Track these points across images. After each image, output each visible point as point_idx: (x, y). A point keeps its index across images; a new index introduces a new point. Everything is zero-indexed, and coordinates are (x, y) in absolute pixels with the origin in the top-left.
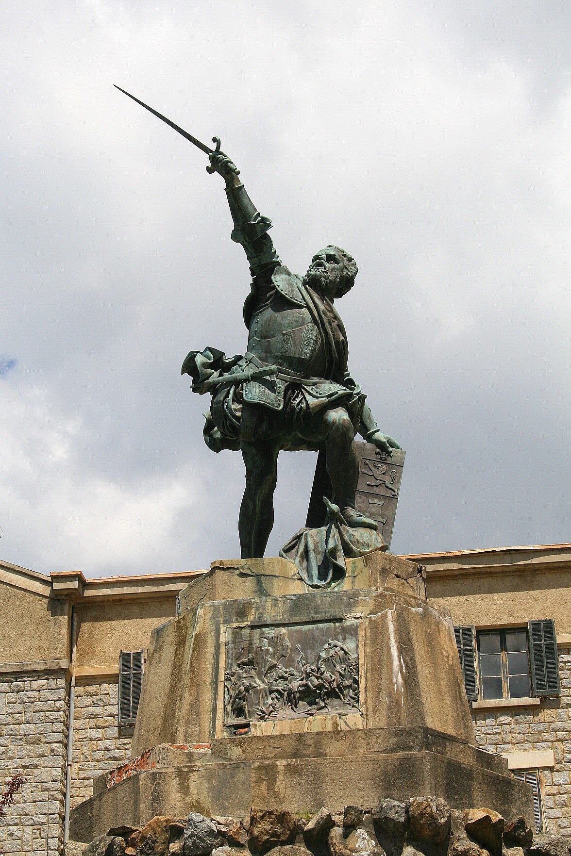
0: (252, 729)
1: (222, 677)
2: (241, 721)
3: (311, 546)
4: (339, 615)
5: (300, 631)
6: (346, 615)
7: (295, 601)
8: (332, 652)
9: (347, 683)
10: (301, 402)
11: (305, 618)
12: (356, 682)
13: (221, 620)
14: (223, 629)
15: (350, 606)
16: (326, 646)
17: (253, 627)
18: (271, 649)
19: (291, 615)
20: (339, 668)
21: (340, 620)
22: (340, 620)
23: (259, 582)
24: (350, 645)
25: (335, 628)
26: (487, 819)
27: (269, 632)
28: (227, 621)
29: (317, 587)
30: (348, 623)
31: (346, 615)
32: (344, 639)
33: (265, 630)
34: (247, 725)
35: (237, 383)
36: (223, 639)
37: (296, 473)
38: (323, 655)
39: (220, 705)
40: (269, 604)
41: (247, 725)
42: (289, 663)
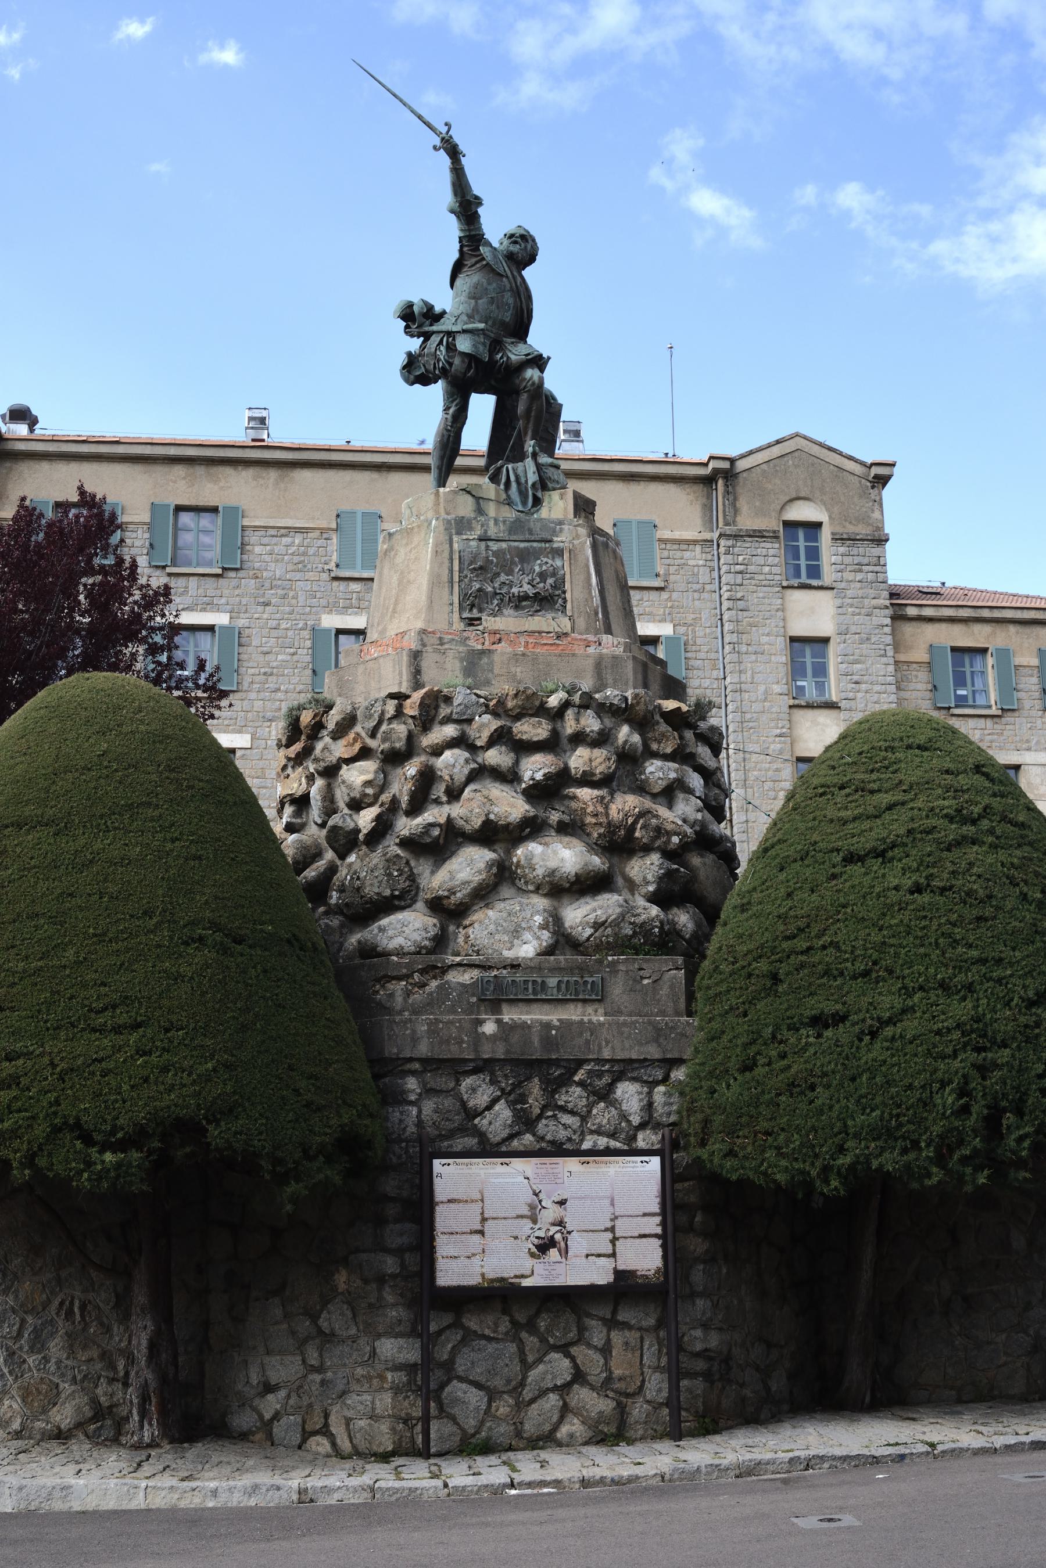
0: (484, 623)
1: (456, 578)
2: (475, 613)
3: (512, 478)
4: (549, 538)
5: (517, 548)
6: (555, 539)
7: (513, 522)
8: (544, 568)
9: (557, 593)
10: (502, 358)
11: (521, 538)
12: (564, 592)
13: (454, 531)
14: (455, 538)
15: (554, 533)
16: (539, 562)
17: (480, 540)
18: (495, 560)
19: (510, 534)
20: (550, 581)
21: (550, 541)
22: (550, 541)
23: (478, 503)
24: (558, 563)
25: (546, 548)
26: (679, 708)
27: (494, 546)
28: (459, 533)
29: (522, 512)
30: (555, 545)
31: (555, 539)
32: (553, 559)
33: (490, 543)
34: (480, 619)
35: (449, 334)
36: (456, 546)
37: (482, 407)
38: (537, 569)
39: (456, 601)
40: (492, 523)
41: (480, 619)
42: (510, 572)
